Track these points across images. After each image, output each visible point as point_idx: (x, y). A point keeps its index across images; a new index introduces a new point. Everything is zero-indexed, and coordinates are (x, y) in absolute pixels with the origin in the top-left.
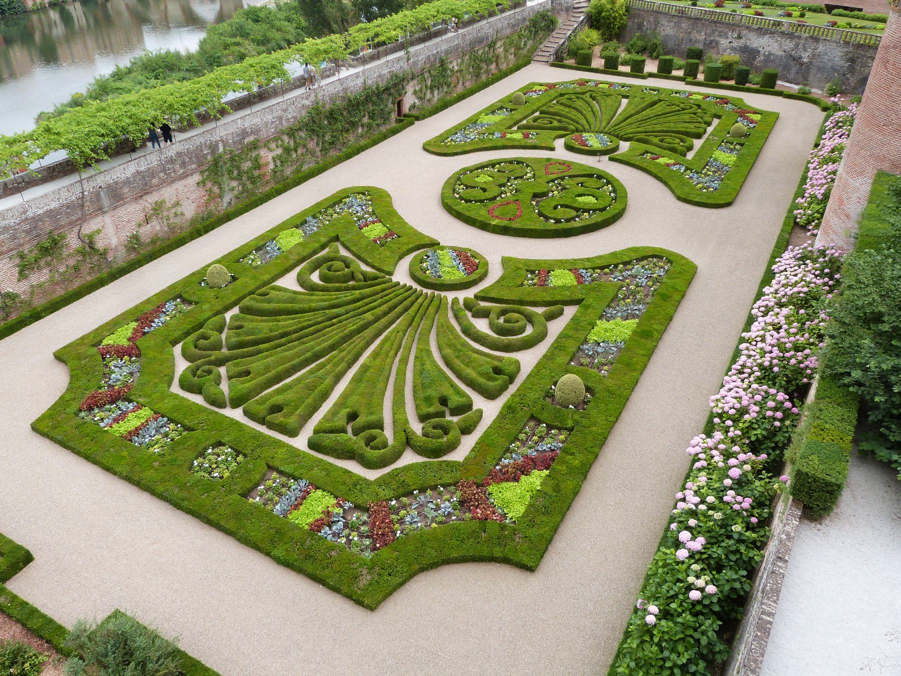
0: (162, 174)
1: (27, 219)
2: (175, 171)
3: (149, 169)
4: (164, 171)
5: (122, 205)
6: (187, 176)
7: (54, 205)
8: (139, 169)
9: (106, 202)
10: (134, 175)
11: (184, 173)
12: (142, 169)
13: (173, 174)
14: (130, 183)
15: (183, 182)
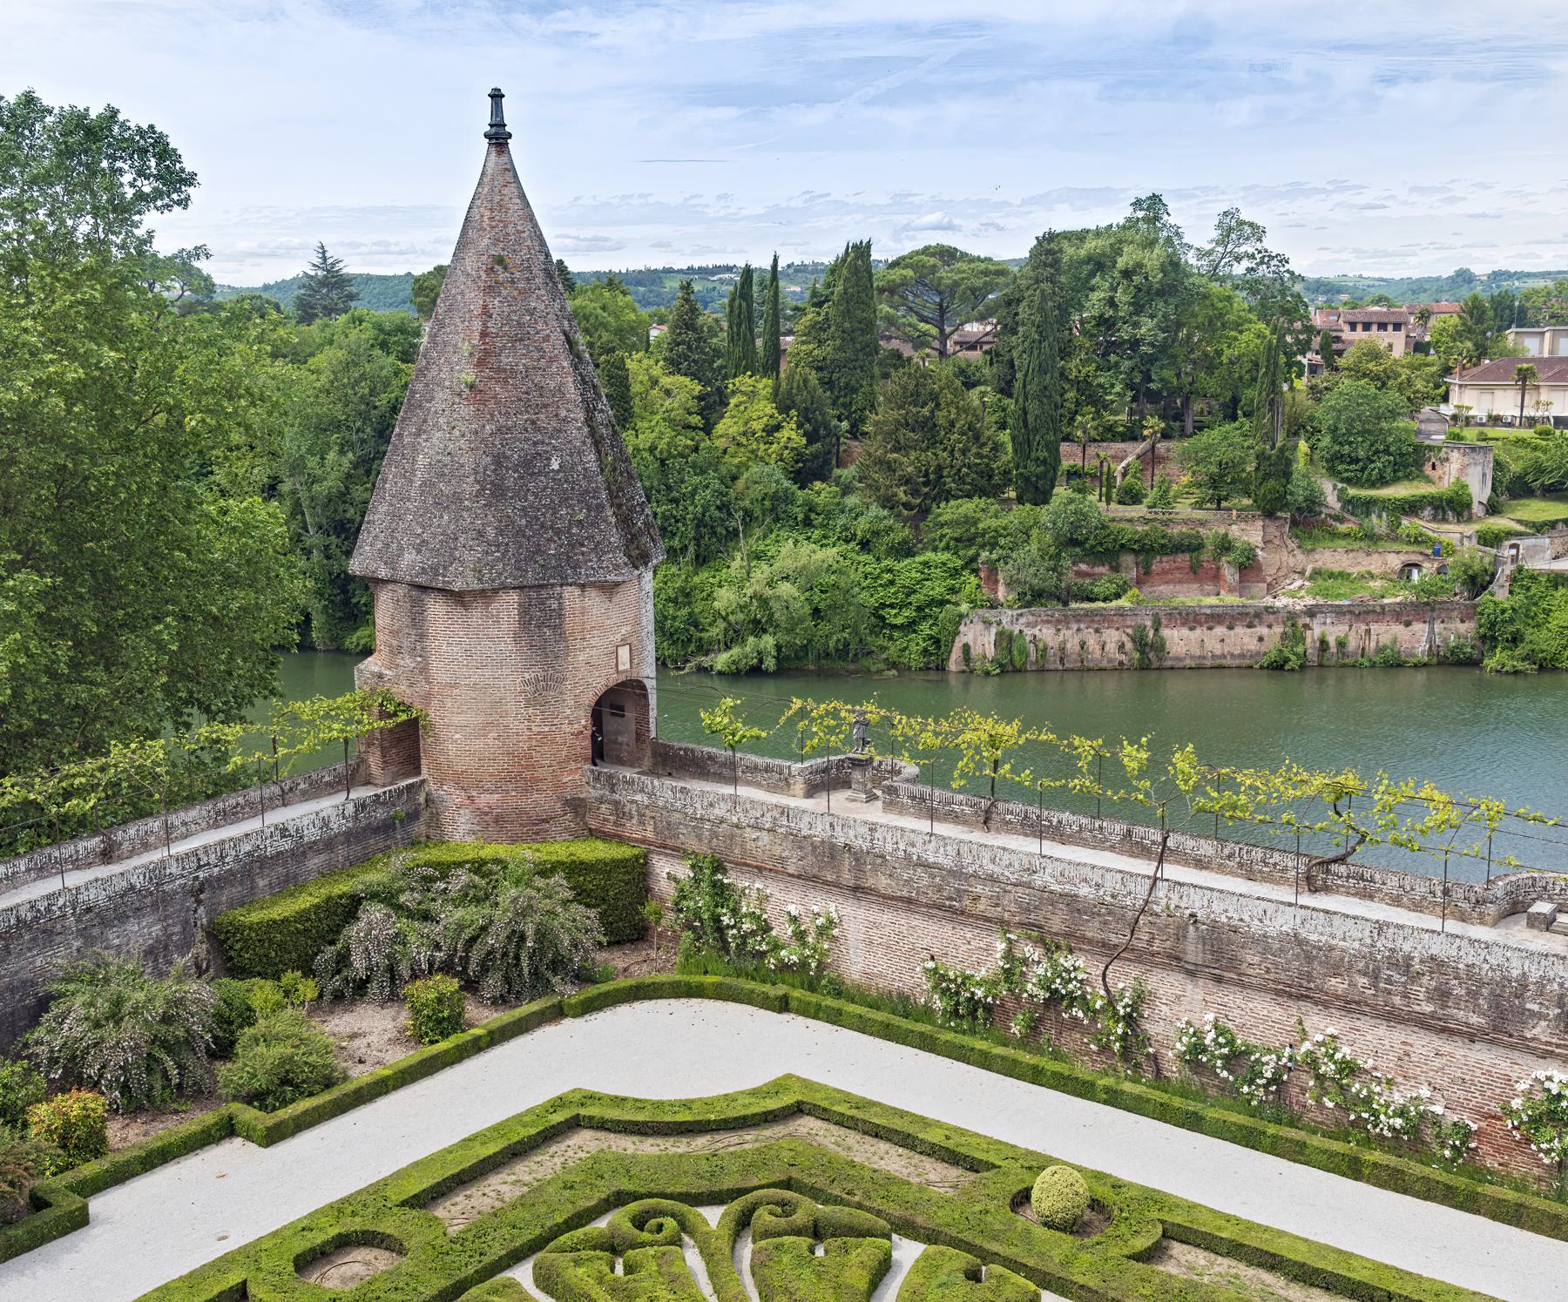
0: (1362, 981)
1: (1029, 886)
2: (1405, 996)
3: (1332, 948)
4: (1375, 977)
5: (1231, 982)
6: (1444, 1030)
7: (1084, 891)
8: (1303, 933)
9: (1193, 952)
10: (1283, 937)
11: (1433, 1016)
12: (1313, 937)
13: (1397, 1000)
14: (1267, 950)
15: (1438, 1042)
